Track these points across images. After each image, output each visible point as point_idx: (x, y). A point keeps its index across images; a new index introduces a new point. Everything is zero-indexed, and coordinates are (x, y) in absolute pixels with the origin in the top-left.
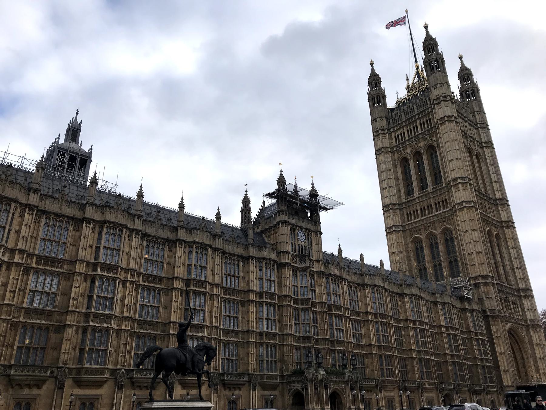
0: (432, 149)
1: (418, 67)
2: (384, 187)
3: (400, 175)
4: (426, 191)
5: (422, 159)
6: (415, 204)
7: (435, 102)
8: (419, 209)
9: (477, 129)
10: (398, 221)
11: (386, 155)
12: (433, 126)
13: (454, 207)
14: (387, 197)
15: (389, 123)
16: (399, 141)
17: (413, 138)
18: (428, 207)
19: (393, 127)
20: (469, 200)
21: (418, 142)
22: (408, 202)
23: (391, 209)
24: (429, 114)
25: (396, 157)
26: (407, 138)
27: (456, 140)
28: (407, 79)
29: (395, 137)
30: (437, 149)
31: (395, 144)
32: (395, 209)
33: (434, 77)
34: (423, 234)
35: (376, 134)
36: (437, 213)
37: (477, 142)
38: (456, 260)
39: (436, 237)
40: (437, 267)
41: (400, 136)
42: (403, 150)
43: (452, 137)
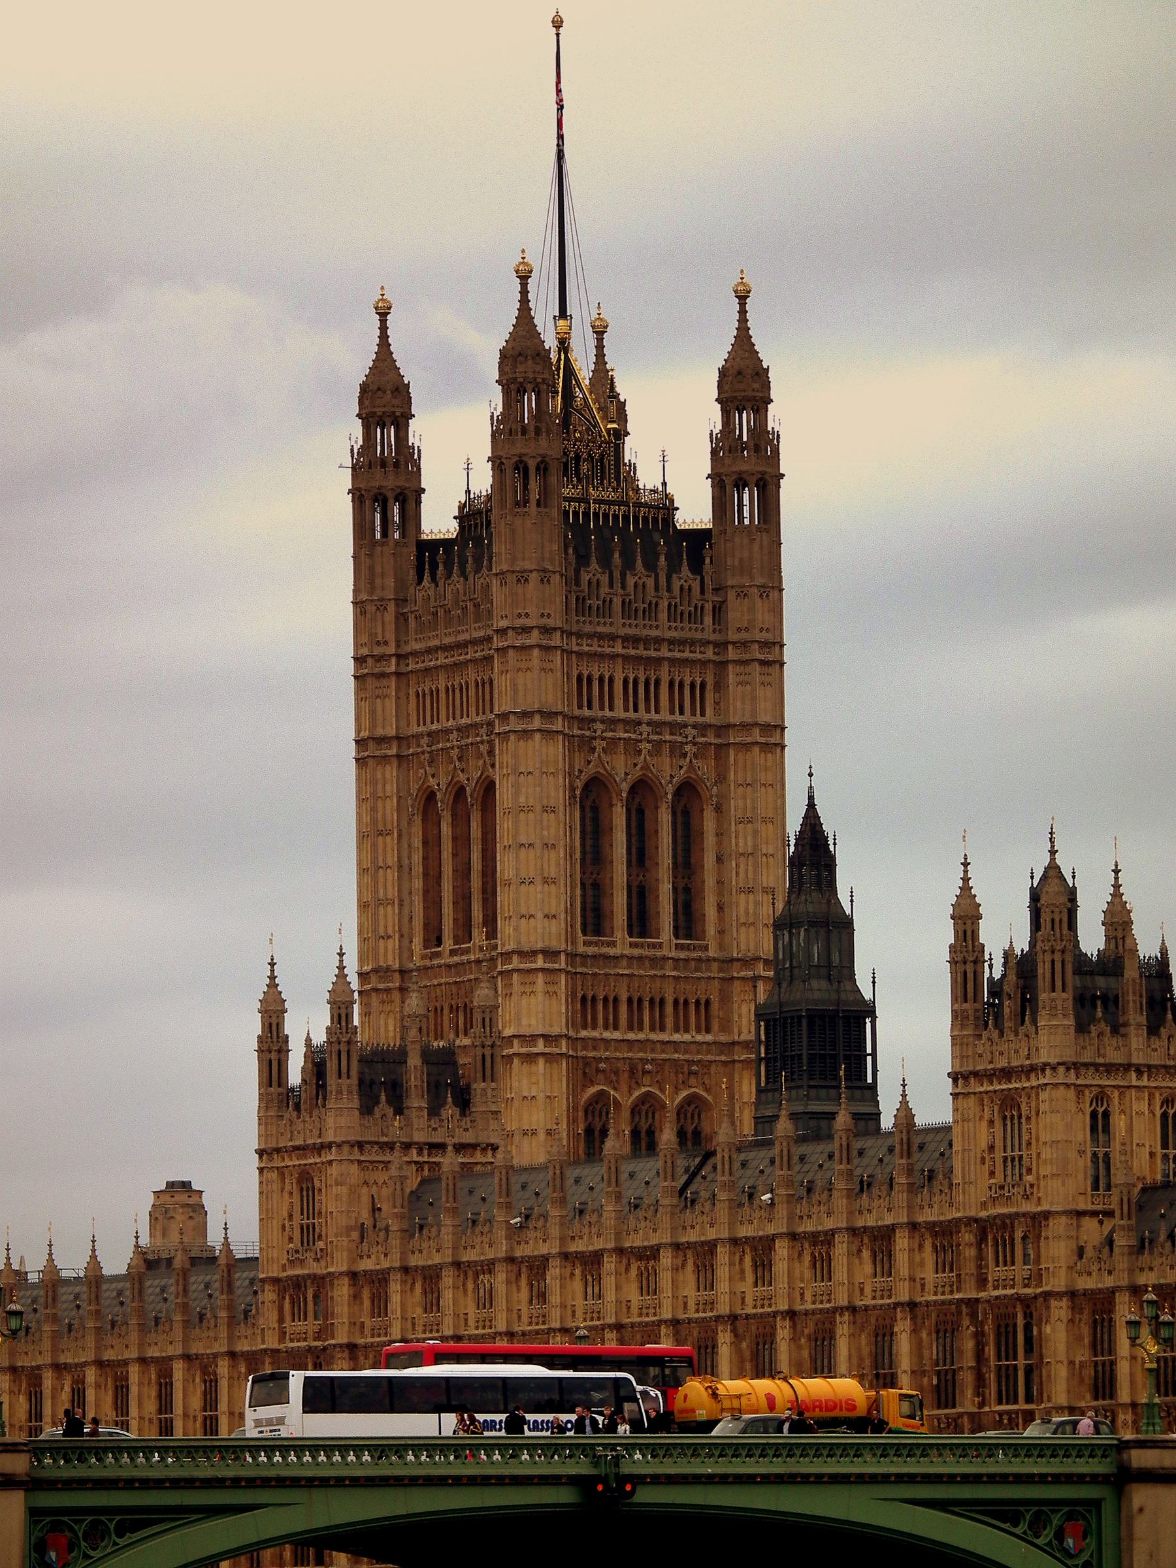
4: (654, 946)
6: (618, 974)
8: (624, 997)
12: (710, 717)
17: (645, 728)
18: (652, 1001)
19: (579, 635)
21: (657, 746)
22: (594, 957)
24: (704, 663)
31: (577, 712)
34: (625, 1088)
36: (677, 1037)
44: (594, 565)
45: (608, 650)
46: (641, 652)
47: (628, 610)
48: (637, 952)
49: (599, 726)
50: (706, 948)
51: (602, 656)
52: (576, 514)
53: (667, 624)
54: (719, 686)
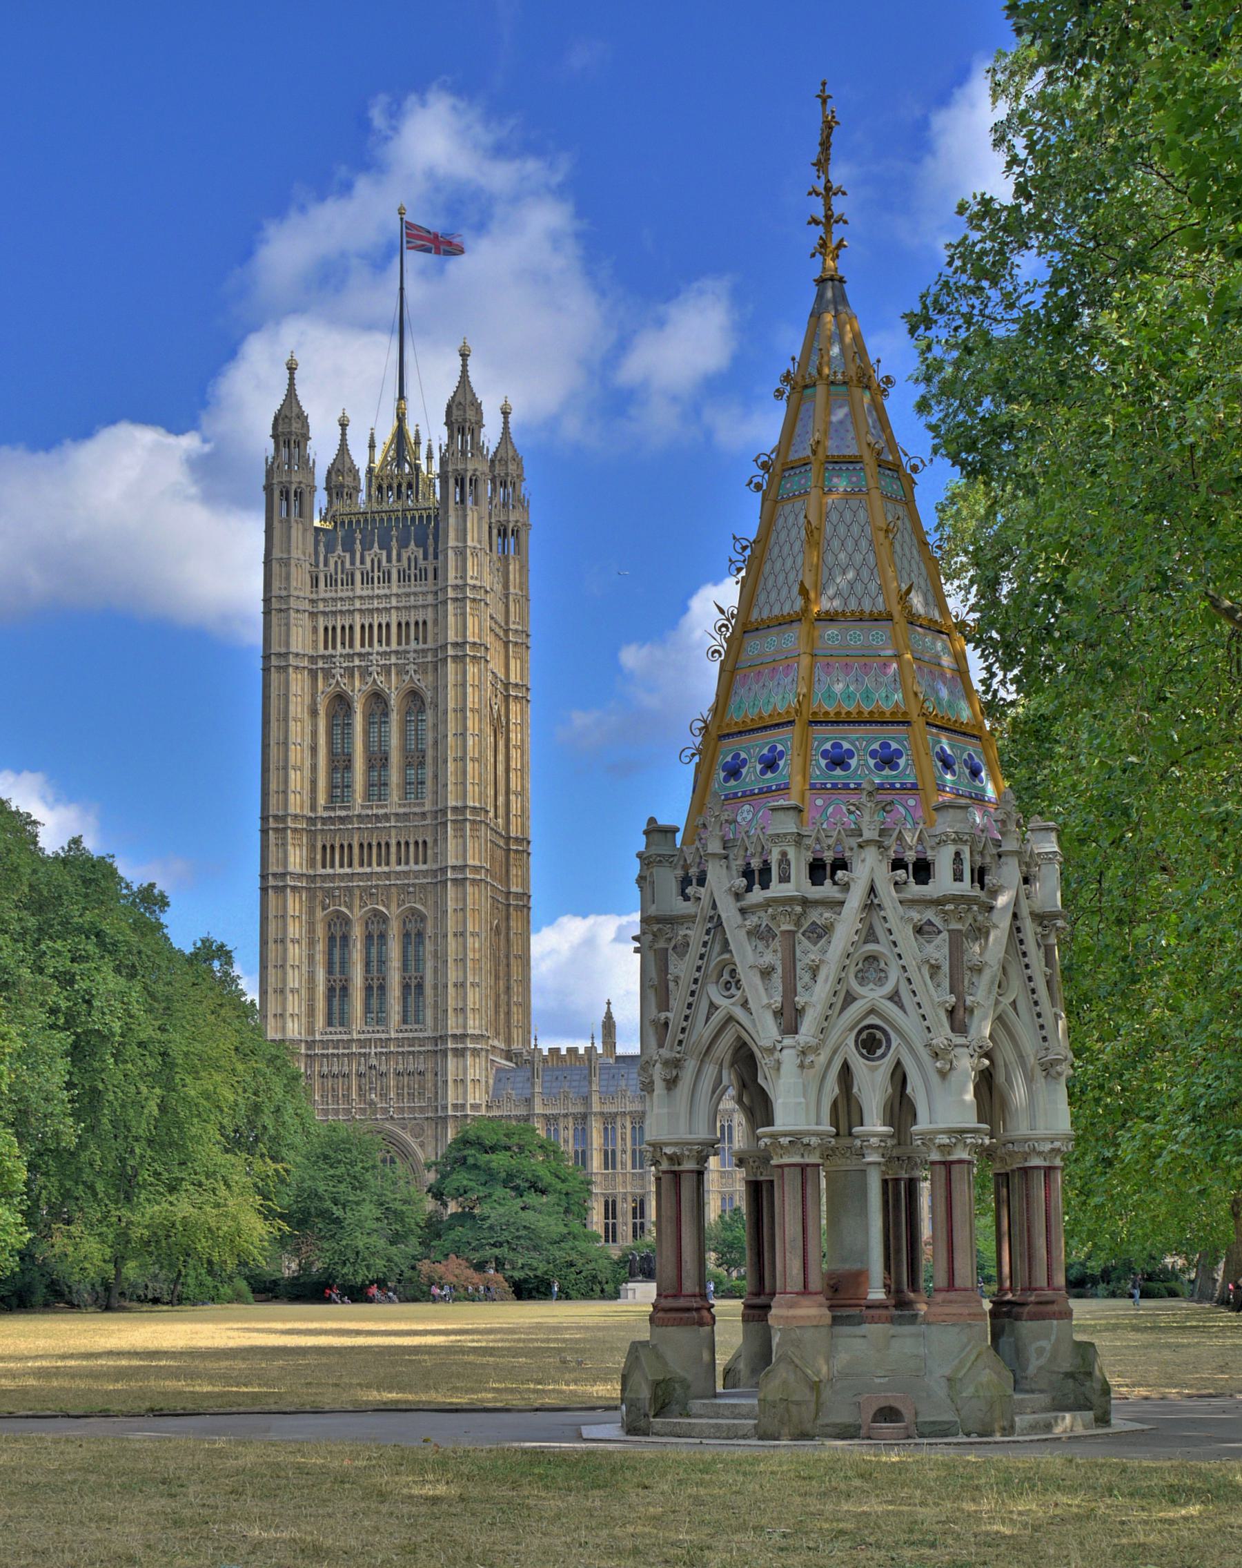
1: (404, 414)
9: (506, 643)
12: (430, 645)
13: (444, 870)
15: (315, 582)
20: (477, 863)
24: (424, 606)
26: (358, 648)
28: (372, 446)
29: (326, 629)
30: (429, 712)
31: (321, 651)
38: (420, 987)
39: (384, 919)
40: (376, 990)
41: (339, 631)
47: (367, 579)
50: (423, 805)
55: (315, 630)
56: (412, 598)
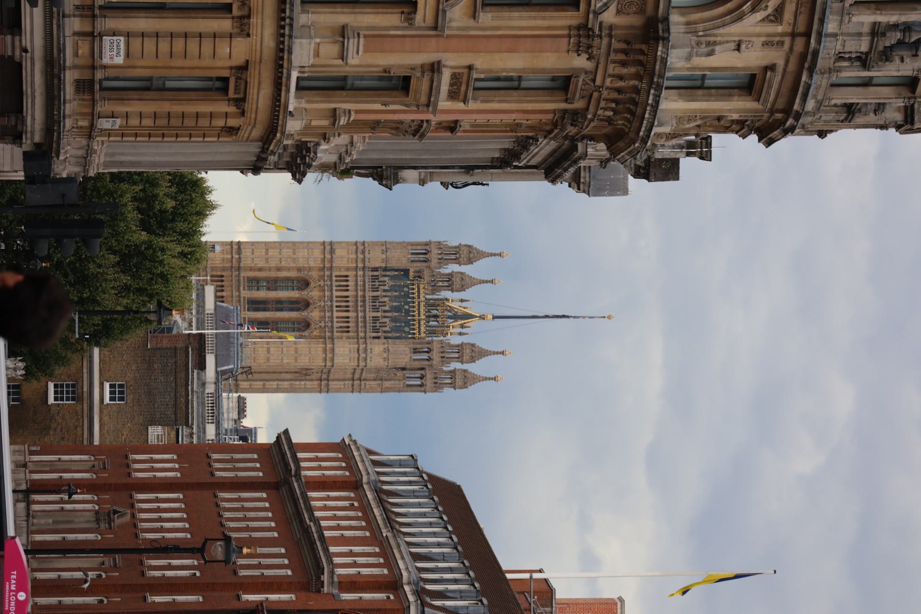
0: (303, 326)
2: (269, 250)
3: (284, 274)
4: (244, 308)
5: (298, 310)
7: (362, 346)
8: (224, 294)
10: (214, 262)
11: (320, 259)
14: (253, 253)
15: (375, 269)
16: (336, 281)
17: (330, 304)
19: (364, 276)
23: (232, 257)
24: (357, 332)
25: (315, 274)
27: (296, 361)
29: (347, 276)
31: (334, 274)
32: (232, 262)
33: (404, 351)
35: (360, 248)
37: (328, 376)
42: (320, 285)
43: (302, 358)
44: (391, 283)
45: (359, 288)
46: (360, 304)
47: (375, 298)
48: (242, 299)
49: (329, 283)
51: (357, 285)
52: (413, 293)
53: (371, 316)
54: (349, 338)
55: (348, 269)
56: (363, 324)
